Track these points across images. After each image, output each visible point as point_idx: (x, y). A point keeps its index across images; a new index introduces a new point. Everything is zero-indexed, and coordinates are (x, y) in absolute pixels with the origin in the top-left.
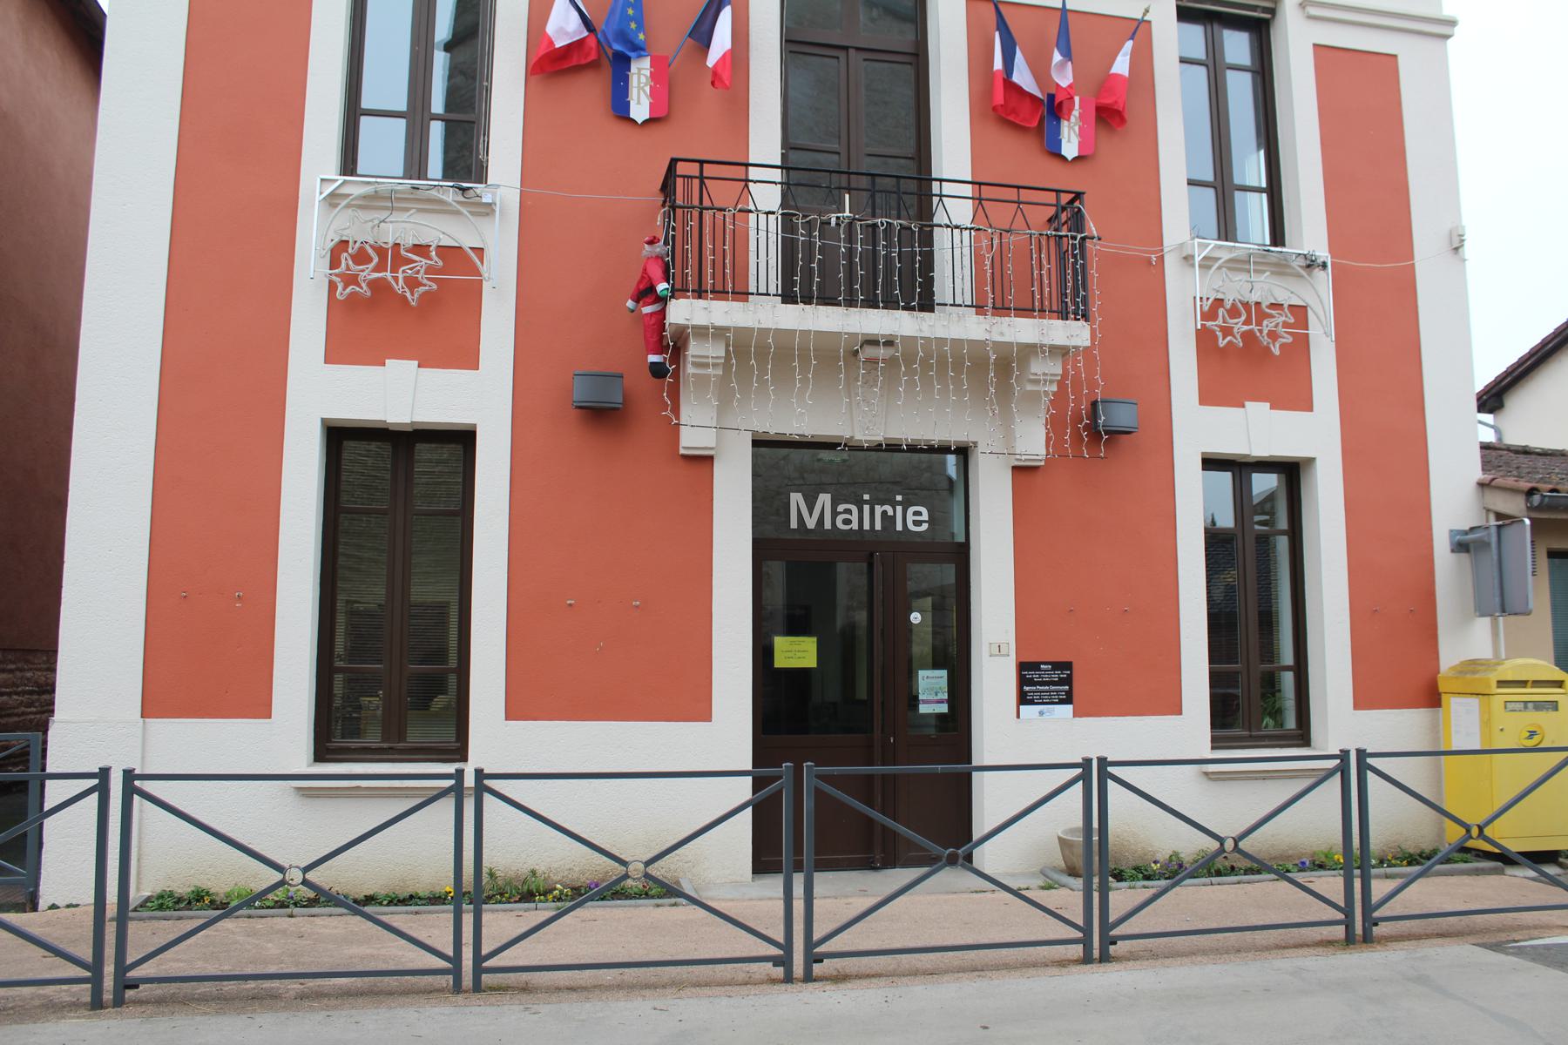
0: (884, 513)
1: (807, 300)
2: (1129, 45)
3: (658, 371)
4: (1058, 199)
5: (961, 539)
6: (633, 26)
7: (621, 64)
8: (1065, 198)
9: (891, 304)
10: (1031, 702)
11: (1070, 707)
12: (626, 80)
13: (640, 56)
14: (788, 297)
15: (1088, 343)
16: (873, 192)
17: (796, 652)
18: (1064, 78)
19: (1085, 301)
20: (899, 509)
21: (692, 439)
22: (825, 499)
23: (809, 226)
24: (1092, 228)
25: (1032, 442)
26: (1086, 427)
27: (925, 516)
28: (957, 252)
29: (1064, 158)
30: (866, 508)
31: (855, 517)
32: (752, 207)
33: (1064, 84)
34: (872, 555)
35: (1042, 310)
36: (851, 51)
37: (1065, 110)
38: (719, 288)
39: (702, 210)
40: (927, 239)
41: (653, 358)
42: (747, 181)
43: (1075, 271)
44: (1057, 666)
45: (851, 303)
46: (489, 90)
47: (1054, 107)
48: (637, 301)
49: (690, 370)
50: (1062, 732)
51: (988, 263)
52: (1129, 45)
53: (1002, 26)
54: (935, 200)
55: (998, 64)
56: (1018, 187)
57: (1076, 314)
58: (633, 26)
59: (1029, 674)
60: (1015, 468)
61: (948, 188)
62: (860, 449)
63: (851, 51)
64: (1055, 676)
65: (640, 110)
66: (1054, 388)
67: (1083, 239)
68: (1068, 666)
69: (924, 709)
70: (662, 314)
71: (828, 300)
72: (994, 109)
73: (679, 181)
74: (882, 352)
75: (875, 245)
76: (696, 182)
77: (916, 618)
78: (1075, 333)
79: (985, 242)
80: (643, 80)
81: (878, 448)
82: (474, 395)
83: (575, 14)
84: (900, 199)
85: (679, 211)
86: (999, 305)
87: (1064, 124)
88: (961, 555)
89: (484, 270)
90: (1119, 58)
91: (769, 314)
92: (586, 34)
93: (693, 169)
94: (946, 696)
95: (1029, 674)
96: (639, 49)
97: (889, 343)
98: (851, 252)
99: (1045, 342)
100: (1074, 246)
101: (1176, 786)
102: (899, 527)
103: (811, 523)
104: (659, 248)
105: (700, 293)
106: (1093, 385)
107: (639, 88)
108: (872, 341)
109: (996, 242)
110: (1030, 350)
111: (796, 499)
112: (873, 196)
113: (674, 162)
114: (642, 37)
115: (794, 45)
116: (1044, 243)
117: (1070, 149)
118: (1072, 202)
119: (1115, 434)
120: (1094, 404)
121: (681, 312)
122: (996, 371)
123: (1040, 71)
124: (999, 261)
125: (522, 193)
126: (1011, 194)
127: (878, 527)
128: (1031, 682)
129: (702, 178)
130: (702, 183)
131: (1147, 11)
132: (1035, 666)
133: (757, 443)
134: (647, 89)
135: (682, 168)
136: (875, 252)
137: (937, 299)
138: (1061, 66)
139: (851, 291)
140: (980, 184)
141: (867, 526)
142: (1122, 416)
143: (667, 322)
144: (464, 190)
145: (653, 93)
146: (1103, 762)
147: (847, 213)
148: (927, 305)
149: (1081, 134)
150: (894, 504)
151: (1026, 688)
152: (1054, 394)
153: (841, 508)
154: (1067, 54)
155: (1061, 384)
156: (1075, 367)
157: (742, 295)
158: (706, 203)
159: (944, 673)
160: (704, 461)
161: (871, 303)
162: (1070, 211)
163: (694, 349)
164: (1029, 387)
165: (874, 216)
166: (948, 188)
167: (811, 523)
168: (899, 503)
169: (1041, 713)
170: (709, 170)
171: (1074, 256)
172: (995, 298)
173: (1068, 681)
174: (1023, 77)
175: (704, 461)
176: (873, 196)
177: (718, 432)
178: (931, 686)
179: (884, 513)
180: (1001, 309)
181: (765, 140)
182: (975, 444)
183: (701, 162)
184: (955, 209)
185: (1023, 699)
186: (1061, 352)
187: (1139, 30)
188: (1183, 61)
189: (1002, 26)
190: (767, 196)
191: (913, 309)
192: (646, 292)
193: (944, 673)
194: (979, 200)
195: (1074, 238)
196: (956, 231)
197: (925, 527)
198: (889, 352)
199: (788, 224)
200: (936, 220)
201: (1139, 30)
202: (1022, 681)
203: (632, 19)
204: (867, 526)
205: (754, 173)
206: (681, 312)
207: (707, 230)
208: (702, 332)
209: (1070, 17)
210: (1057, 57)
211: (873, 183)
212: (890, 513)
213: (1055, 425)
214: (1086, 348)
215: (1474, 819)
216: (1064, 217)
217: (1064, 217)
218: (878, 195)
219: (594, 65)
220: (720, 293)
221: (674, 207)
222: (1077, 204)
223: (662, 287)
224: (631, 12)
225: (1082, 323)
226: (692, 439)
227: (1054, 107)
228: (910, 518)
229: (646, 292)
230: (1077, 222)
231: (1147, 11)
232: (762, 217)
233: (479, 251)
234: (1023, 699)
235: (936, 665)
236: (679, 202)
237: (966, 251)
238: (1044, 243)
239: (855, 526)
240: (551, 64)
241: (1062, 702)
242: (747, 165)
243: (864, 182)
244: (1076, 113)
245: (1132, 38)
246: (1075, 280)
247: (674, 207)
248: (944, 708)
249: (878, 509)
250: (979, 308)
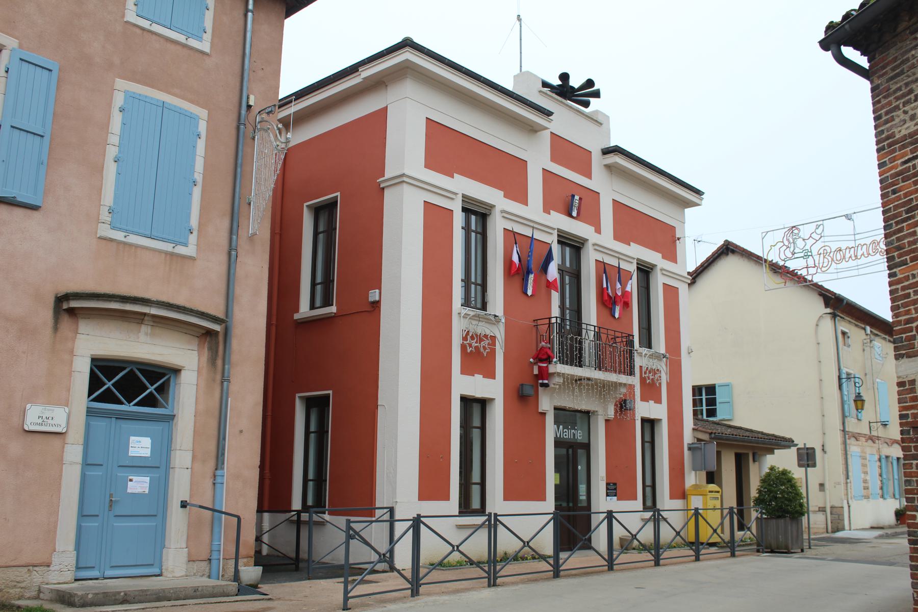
25: (611, 413)
50: (613, 504)
55: (605, 286)
68: (615, 484)
77: (579, 467)
82: (492, 388)
88: (587, 447)
101: (447, 527)
110: (620, 384)
122: (603, 388)
146: (496, 515)
160: (543, 414)
173: (615, 489)
175: (543, 414)
177: (546, 404)
185: (607, 495)
189: (605, 272)
202: (607, 489)
208: (559, 374)
215: (526, 540)
234: (607, 495)
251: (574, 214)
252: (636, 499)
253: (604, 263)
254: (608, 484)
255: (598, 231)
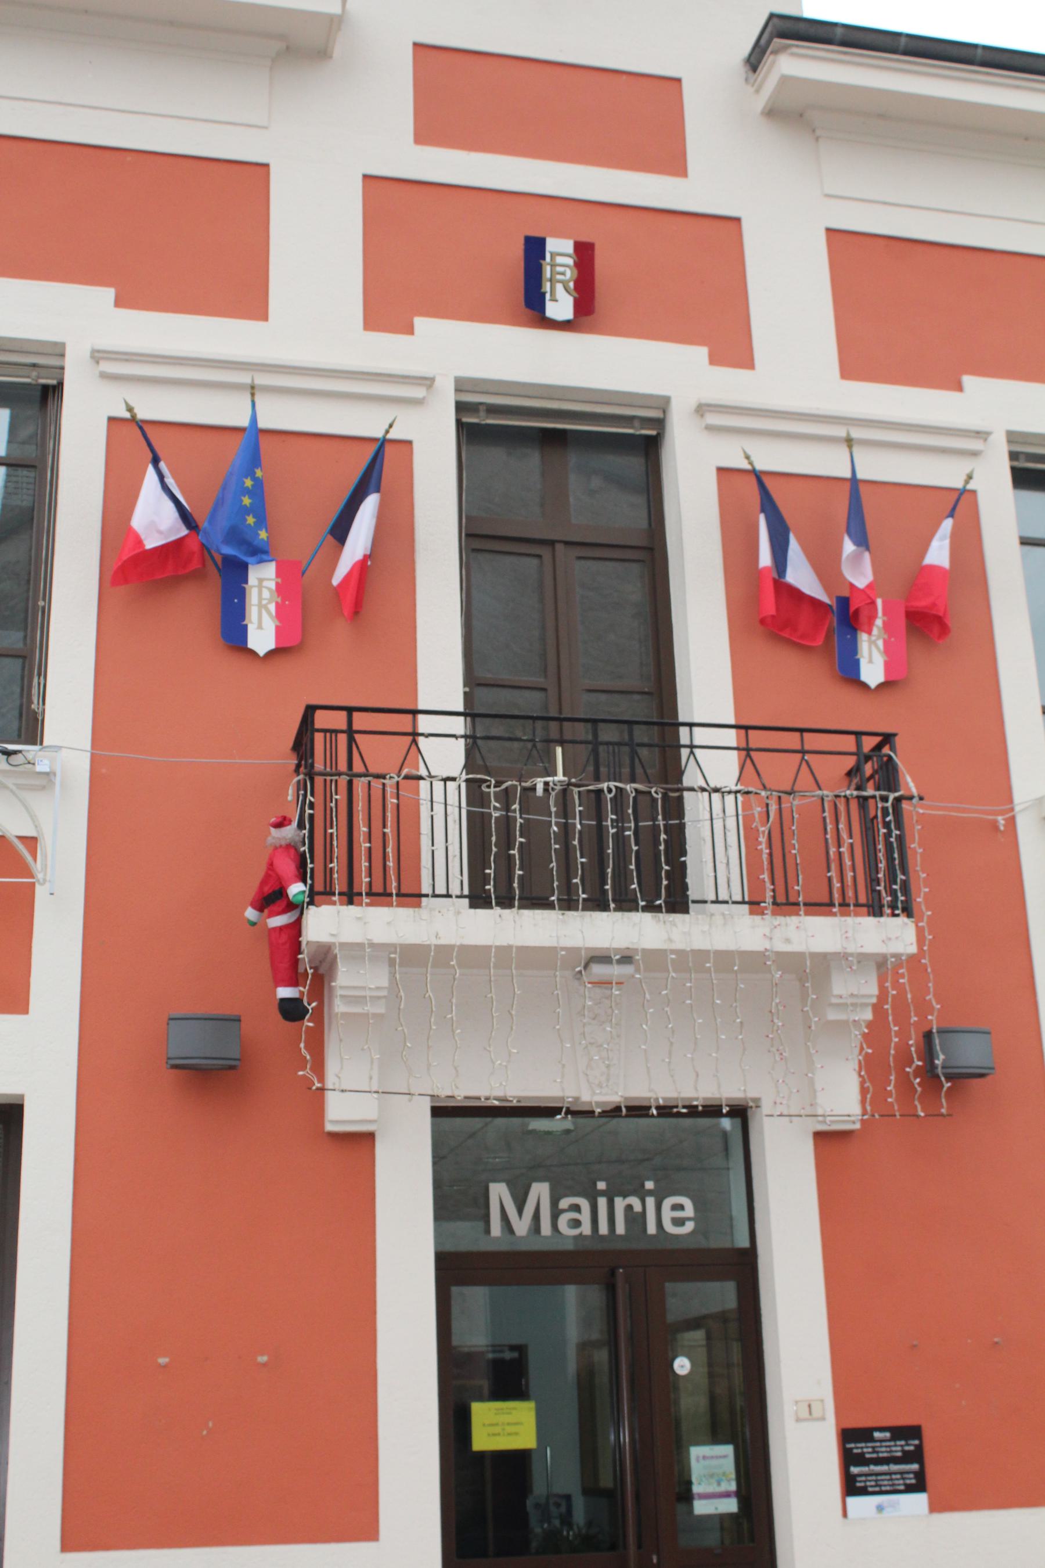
0: (629, 1208)
1: (506, 902)
2: (947, 524)
3: (292, 1010)
4: (859, 745)
5: (744, 1243)
6: (251, 520)
7: (235, 574)
8: (869, 743)
9: (626, 903)
10: (863, 1492)
11: (919, 1501)
12: (242, 595)
13: (261, 561)
14: (478, 899)
15: (913, 949)
16: (595, 744)
17: (504, 1426)
18: (860, 574)
19: (905, 888)
20: (650, 1202)
21: (342, 1112)
22: (540, 1191)
23: (506, 798)
24: (909, 784)
25: (842, 1098)
26: (918, 1072)
27: (689, 1211)
28: (718, 825)
29: (864, 686)
30: (602, 1202)
31: (585, 1217)
32: (423, 772)
33: (861, 583)
34: (613, 1272)
35: (844, 904)
36: (559, 547)
37: (863, 618)
38: (378, 888)
39: (352, 776)
40: (675, 808)
41: (285, 992)
42: (415, 734)
43: (889, 846)
44: (900, 1433)
45: (568, 904)
46: (46, 612)
47: (850, 614)
48: (260, 909)
49: (339, 1007)
51: (763, 839)
52: (947, 524)
53: (768, 505)
54: (685, 752)
55: (765, 558)
56: (801, 731)
57: (893, 906)
58: (251, 520)
59: (857, 1448)
60: (820, 1137)
61: (701, 736)
62: (590, 1113)
63: (559, 547)
64: (897, 1448)
65: (262, 636)
66: (868, 1015)
67: (898, 800)
68: (913, 1432)
69: (701, 1508)
70: (296, 928)
71: (536, 901)
72: (762, 622)
73: (319, 737)
74: (615, 971)
75: (600, 817)
76: (343, 738)
77: (682, 1365)
78: (894, 936)
79: (758, 810)
80: (266, 594)
81: (615, 1112)
83: (170, 506)
84: (633, 754)
85: (319, 780)
86: (781, 899)
87: (863, 638)
88: (743, 1267)
89: (37, 867)
90: (935, 544)
91: (450, 922)
92: (184, 532)
93: (338, 720)
94: (733, 1487)
95: (857, 1448)
96: (260, 553)
97: (626, 959)
98: (566, 830)
99: (852, 948)
100: (885, 811)
102: (652, 1229)
103: (521, 1226)
104: (290, 832)
105: (350, 897)
106: (923, 1008)
107: (261, 606)
108: (602, 958)
109: (773, 808)
111: (499, 1192)
112: (595, 752)
113: (310, 711)
114: (263, 535)
115: (478, 539)
116: (842, 807)
117: (872, 670)
118: (878, 747)
119: (959, 1077)
120: (928, 1036)
121: (325, 924)
123: (826, 565)
124: (779, 838)
125: (93, 757)
126: (792, 740)
127: (620, 1229)
128: (862, 1460)
129: (351, 733)
130: (351, 741)
131: (970, 477)
132: (864, 1434)
133: (438, 1112)
134: (272, 607)
135: (322, 720)
136: (600, 829)
137: (693, 894)
138: (856, 558)
139: (568, 888)
140: (747, 728)
141: (603, 1229)
142: (970, 1053)
143: (304, 940)
144: (8, 754)
145: (281, 613)
147: (560, 777)
148: (678, 901)
149: (888, 650)
150: (643, 1195)
151: (855, 1470)
152: (870, 1025)
153: (564, 1203)
154: (862, 541)
155: (877, 1009)
156: (896, 984)
157: (412, 897)
158: (358, 767)
159: (728, 1450)
160: (361, 1143)
161: (598, 903)
162: (876, 764)
163: (345, 978)
164: (832, 1015)
165: (597, 778)
166: (701, 736)
167: (521, 1226)
168: (650, 1193)
169: (880, 1508)
170: (361, 721)
171: (887, 825)
172: (776, 890)
173: (916, 1455)
174: (801, 575)
175: (361, 1143)
176: (595, 752)
178: (711, 1471)
179: (629, 1208)
180: (786, 905)
181: (440, 676)
182: (757, 1101)
183: (350, 710)
184: (713, 764)
186: (881, 963)
187: (960, 503)
188: (1025, 542)
189: (768, 505)
190: (444, 755)
191: (658, 909)
192: (272, 898)
193: (728, 1450)
194: (746, 751)
195: (885, 799)
196: (716, 796)
197: (689, 1226)
198: (628, 969)
199: (475, 794)
200: (687, 781)
201: (960, 503)
202: (848, 1459)
203: (247, 511)
204: (603, 1229)
205: (424, 724)
206: (325, 924)
207: (360, 806)
209: (862, 488)
210: (849, 547)
211: (595, 735)
212: (638, 1207)
213: (872, 1071)
214: (912, 958)
216: (868, 769)
217: (868, 769)
218: (601, 748)
219: (198, 575)
220: (380, 896)
221: (311, 775)
222: (886, 750)
223: (296, 890)
224: (247, 501)
225: (903, 920)
226: (342, 1112)
227: (850, 614)
228: (667, 1215)
229: (272, 898)
230: (888, 776)
231: (970, 477)
232: (438, 786)
233: (31, 842)
234: (851, 1487)
235: (715, 1438)
236: (319, 766)
237: (731, 823)
238: (842, 807)
239: (586, 1229)
240: (135, 572)
241: (910, 1489)
242: (415, 712)
243: (582, 731)
244: (879, 622)
245: (951, 515)
246: (890, 859)
247: (311, 775)
248: (731, 1506)
249: (620, 1203)
250: (754, 905)
251: (561, 306)
252: (360, 1522)
253: (759, 477)
254: (848, 1436)
255: (734, 348)
